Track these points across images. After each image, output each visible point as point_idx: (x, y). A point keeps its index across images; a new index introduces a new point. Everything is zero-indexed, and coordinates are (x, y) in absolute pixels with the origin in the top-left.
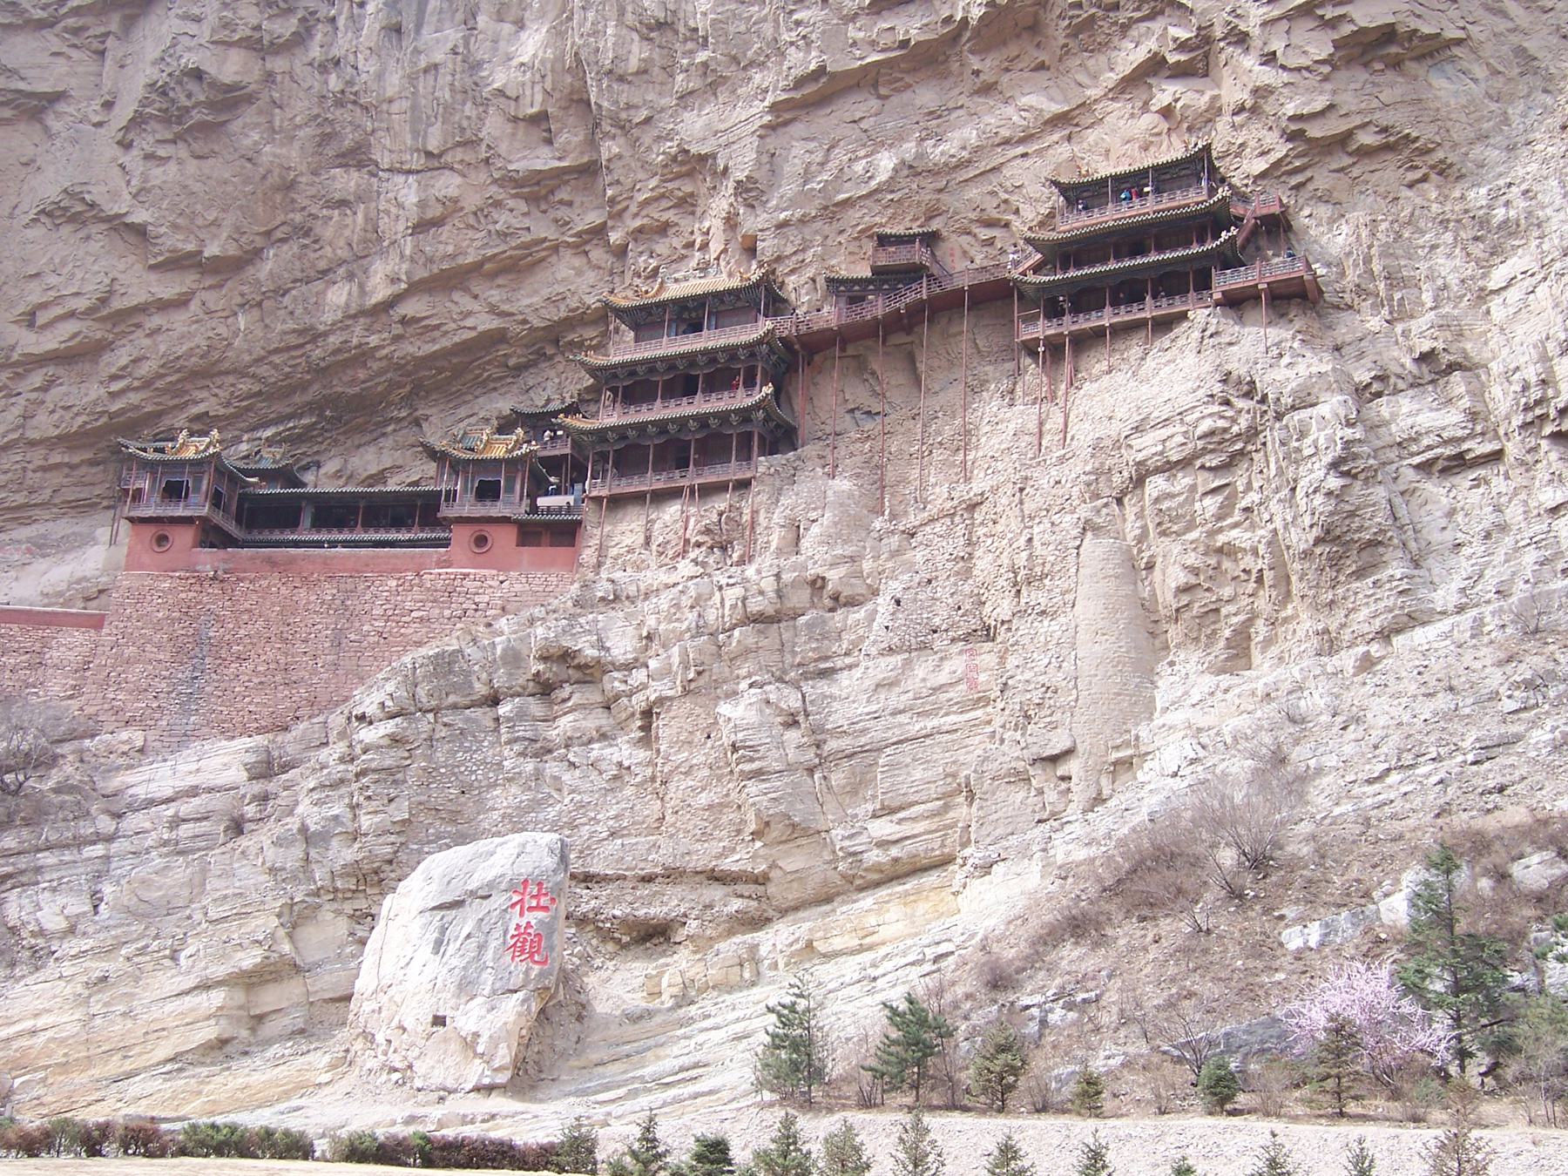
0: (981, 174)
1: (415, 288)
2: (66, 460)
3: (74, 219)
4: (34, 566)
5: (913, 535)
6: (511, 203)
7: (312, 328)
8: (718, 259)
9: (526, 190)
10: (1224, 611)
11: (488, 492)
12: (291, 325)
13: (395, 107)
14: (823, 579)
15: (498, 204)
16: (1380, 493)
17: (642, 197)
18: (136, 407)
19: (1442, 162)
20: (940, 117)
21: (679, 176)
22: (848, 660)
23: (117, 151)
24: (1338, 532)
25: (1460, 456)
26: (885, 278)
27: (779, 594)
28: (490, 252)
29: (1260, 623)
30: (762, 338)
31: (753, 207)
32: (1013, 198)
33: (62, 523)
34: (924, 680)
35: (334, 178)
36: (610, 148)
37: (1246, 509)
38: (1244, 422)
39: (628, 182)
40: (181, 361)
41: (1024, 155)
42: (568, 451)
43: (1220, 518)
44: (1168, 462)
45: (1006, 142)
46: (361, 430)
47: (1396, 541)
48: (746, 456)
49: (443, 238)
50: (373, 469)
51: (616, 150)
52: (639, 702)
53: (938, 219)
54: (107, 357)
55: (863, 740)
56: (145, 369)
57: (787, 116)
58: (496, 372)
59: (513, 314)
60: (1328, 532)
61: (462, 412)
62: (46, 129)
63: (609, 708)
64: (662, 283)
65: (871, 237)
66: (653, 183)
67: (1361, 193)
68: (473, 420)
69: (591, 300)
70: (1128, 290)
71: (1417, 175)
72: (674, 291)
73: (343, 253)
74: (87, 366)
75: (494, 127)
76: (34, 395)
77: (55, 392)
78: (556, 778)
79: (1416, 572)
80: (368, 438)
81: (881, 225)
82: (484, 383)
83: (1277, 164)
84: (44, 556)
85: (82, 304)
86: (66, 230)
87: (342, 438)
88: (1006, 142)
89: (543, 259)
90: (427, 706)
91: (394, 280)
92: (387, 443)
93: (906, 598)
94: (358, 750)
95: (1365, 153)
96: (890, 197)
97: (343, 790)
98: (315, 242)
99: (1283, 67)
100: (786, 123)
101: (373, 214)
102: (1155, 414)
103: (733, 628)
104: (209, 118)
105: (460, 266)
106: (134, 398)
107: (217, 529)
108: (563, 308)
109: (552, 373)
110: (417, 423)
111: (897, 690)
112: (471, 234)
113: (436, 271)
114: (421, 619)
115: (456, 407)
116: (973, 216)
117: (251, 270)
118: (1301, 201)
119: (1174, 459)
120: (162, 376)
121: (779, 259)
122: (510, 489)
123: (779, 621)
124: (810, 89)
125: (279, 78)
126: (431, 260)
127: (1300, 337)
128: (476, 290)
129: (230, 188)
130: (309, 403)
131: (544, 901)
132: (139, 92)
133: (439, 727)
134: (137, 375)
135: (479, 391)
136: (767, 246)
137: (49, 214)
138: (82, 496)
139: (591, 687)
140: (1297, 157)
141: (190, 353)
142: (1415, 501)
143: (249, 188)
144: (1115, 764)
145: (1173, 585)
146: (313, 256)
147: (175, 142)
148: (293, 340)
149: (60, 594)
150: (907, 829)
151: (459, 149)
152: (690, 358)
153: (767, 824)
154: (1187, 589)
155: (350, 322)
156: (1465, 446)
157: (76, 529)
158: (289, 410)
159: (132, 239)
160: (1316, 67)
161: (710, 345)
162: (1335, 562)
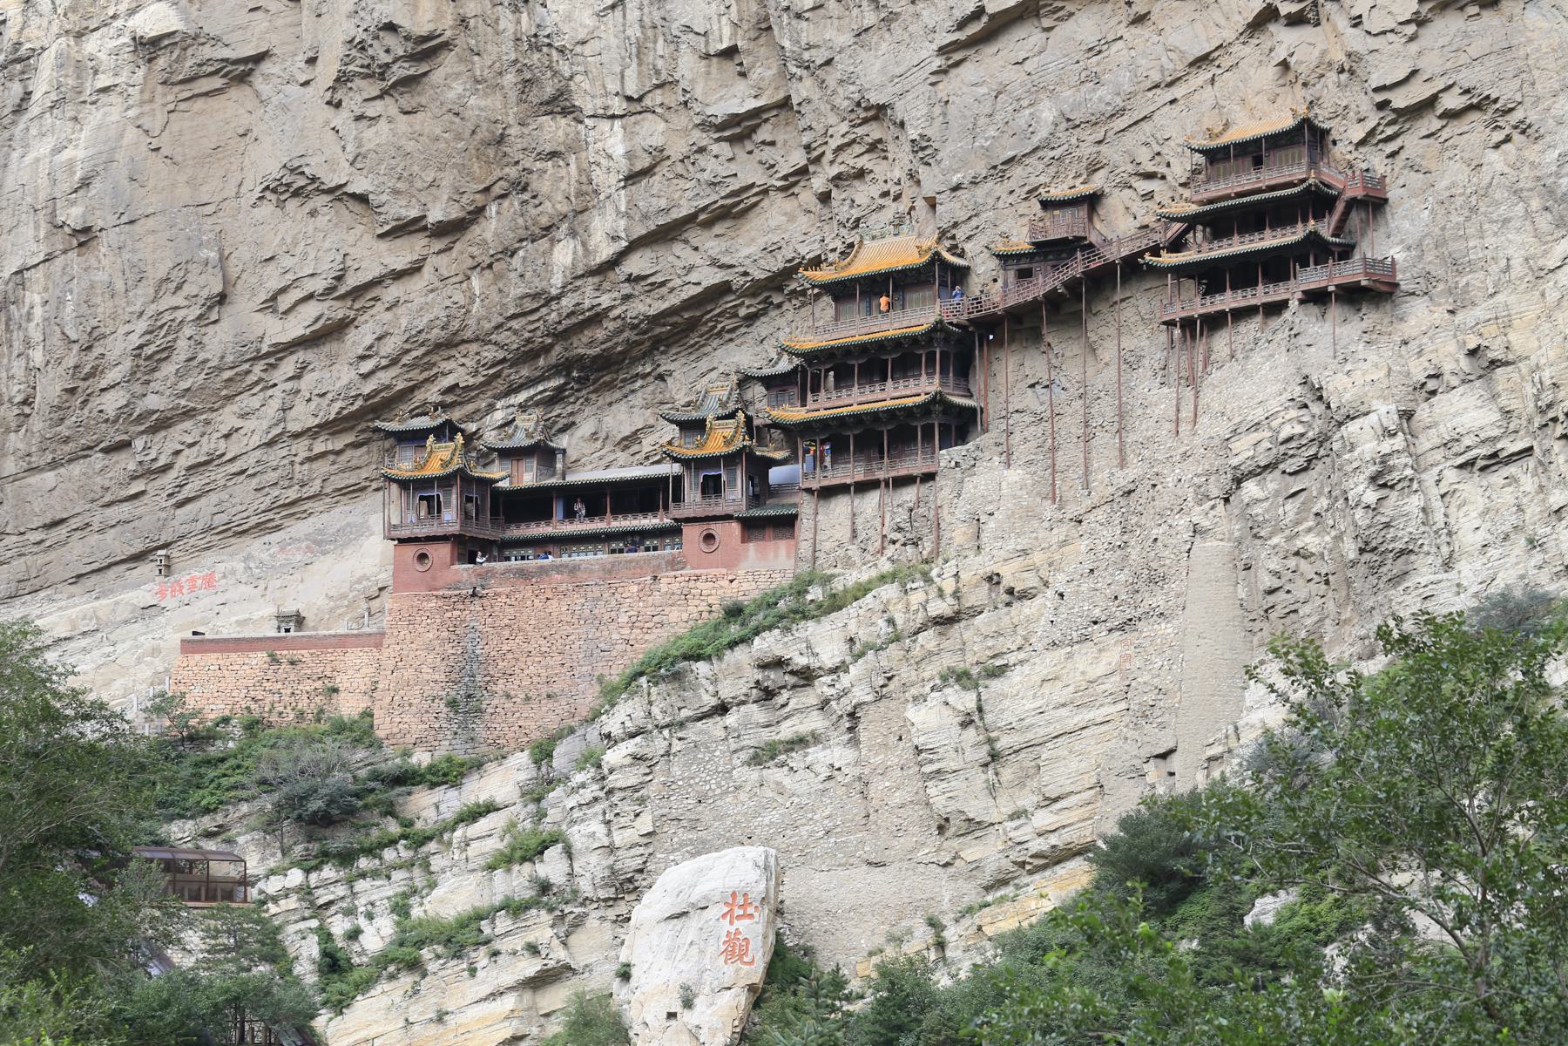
0: (1136, 123)
1: (635, 245)
2: (330, 447)
3: (296, 194)
4: (316, 566)
5: (1080, 522)
6: (715, 148)
8: (909, 213)
9: (727, 134)
10: (1301, 613)
11: (712, 487)
12: (520, 291)
13: (587, 49)
14: (998, 575)
15: (702, 150)
16: (1415, 502)
17: (834, 143)
18: (388, 387)
19: (1522, 122)
20: (1100, 52)
21: (865, 121)
22: (1022, 655)
23: (330, 110)
24: (1374, 544)
25: (1495, 455)
26: (1051, 251)
27: (956, 594)
28: (702, 203)
29: (1327, 621)
32: (1164, 151)
34: (1083, 673)
36: (802, 90)
37: (1317, 514)
38: (1318, 425)
39: (820, 128)
41: (1173, 102)
43: (1298, 523)
44: (1258, 466)
45: (1157, 86)
46: (610, 386)
47: (1426, 548)
51: (804, 94)
52: (845, 705)
53: (1101, 173)
54: (352, 335)
55: (1030, 736)
56: (389, 347)
57: (957, 57)
60: (1367, 543)
61: (704, 365)
62: (258, 95)
66: (844, 127)
67: (1450, 158)
68: (713, 375)
69: (803, 250)
70: (1243, 272)
71: (1498, 136)
73: (564, 208)
75: (688, 66)
76: (288, 386)
77: (309, 379)
78: (778, 784)
79: (1445, 576)
80: (618, 394)
81: (1046, 185)
82: (719, 334)
83: (1372, 133)
84: (324, 553)
85: (319, 285)
86: (292, 204)
87: (593, 397)
88: (1157, 86)
89: (755, 205)
90: (662, 723)
91: (615, 238)
92: (637, 399)
93: (1067, 590)
94: (606, 771)
95: (1451, 115)
96: (1052, 154)
97: (598, 808)
98: (534, 197)
99: (1369, 33)
100: (957, 64)
101: (585, 165)
102: (1249, 418)
104: (411, 72)
106: (384, 377)
108: (780, 257)
109: (781, 322)
110: (661, 377)
111: (1059, 684)
112: (682, 183)
113: (653, 227)
115: (698, 359)
116: (1131, 168)
117: (475, 231)
118: (1397, 169)
119: (1262, 464)
120: (408, 351)
121: (956, 225)
122: (732, 483)
123: (959, 621)
124: (974, 29)
125: (472, 22)
126: (646, 217)
127: (1366, 337)
128: (695, 242)
129: (442, 145)
131: (750, 910)
132: (341, 50)
133: (675, 742)
134: (383, 353)
135: (715, 343)
137: (274, 191)
138: (352, 481)
140: (1391, 123)
142: (1455, 502)
143: (461, 145)
144: (1210, 759)
145: (1262, 588)
146: (534, 212)
147: (380, 97)
149: (344, 596)
150: (1064, 818)
151: (659, 91)
153: (947, 820)
154: (1271, 592)
155: (579, 283)
156: (1499, 446)
157: (350, 519)
158: (538, 373)
159: (357, 207)
160: (1399, 29)
162: (1374, 569)
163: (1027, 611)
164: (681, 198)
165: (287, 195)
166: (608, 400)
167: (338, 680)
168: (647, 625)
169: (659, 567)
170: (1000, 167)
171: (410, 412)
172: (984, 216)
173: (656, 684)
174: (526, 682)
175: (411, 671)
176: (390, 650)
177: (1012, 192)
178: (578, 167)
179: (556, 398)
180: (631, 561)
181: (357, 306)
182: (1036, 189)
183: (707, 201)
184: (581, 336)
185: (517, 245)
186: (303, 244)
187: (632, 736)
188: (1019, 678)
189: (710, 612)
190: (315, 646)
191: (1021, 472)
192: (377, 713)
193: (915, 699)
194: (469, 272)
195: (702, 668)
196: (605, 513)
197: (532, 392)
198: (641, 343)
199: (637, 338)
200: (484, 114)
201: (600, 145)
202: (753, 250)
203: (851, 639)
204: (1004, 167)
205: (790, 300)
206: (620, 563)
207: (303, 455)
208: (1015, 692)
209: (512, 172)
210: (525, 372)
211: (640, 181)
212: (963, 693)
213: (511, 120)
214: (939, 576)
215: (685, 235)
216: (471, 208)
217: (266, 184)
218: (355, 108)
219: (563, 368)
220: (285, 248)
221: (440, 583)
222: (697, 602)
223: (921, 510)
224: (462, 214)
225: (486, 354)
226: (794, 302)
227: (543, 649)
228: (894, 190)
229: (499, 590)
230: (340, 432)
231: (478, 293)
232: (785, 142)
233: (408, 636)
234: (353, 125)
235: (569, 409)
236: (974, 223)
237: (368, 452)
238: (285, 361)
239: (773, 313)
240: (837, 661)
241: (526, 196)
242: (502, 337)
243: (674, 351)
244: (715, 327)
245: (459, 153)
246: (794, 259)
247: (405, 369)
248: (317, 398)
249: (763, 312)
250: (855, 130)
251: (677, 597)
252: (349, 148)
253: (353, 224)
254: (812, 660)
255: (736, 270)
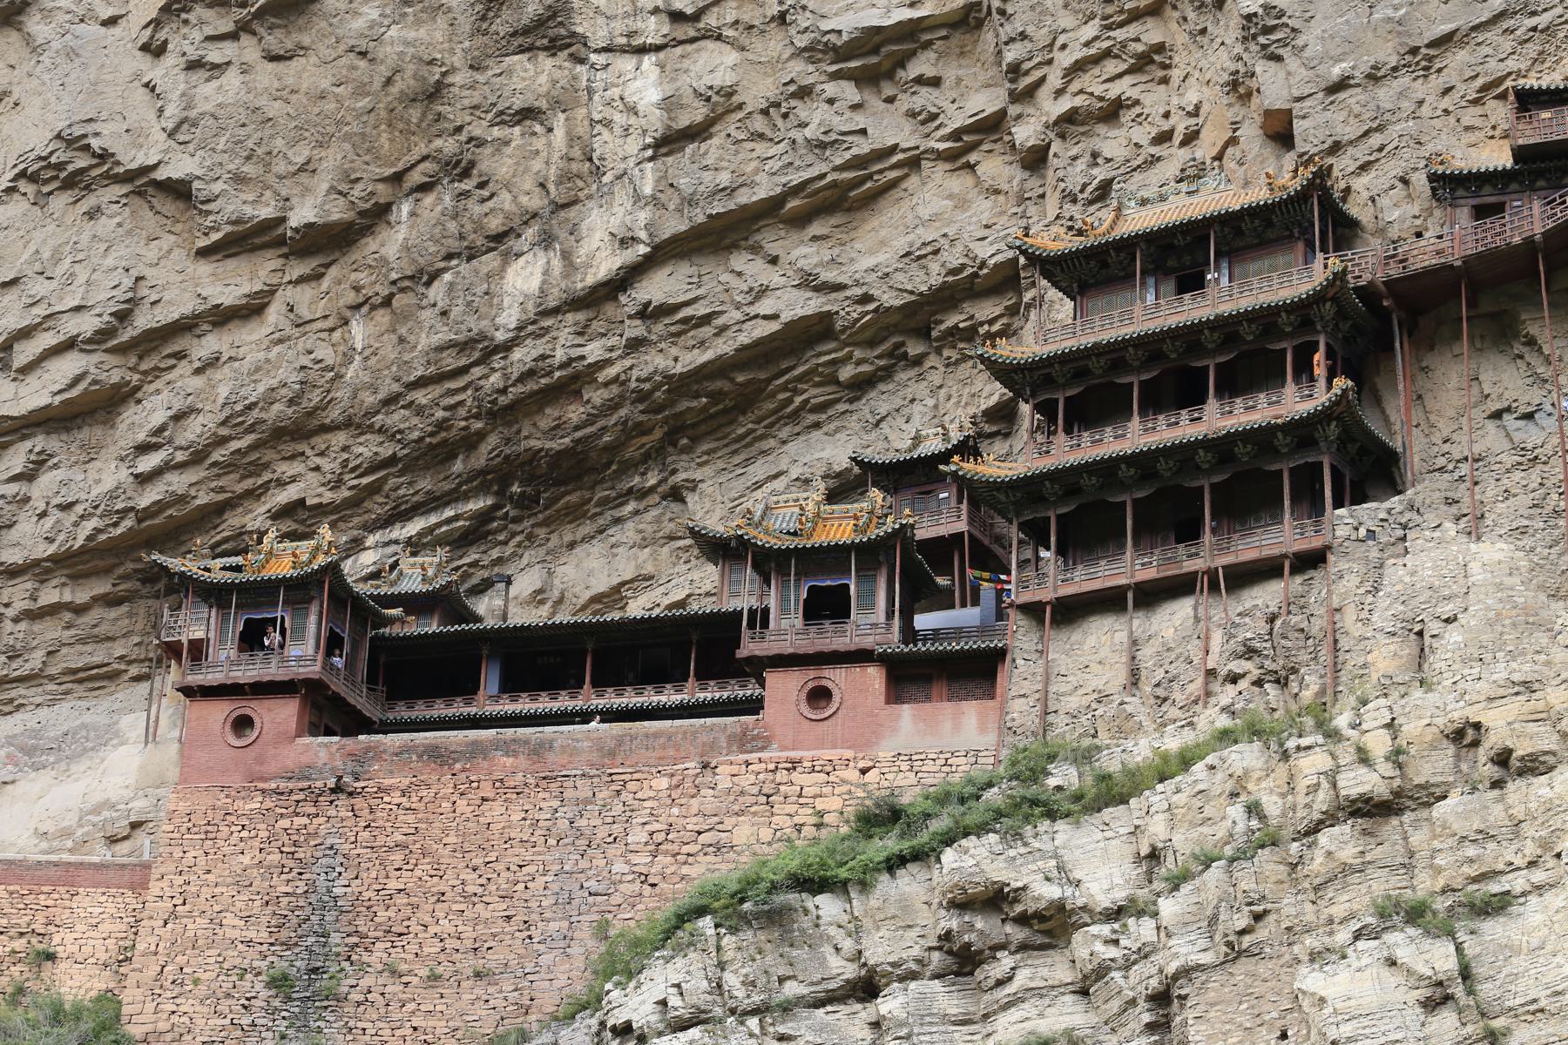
1: (664, 253)
2: (67, 597)
3: (69, 184)
6: (831, 89)
7: (483, 336)
8: (1219, 157)
9: (853, 64)
12: (443, 335)
14: (1477, 726)
15: (804, 93)
17: (1065, 59)
18: (182, 499)
22: (1538, 876)
23: (143, 62)
27: (1396, 756)
28: (796, 178)
30: (1324, 289)
31: (1278, 59)
33: (64, 708)
35: (508, 72)
39: (1041, 36)
40: (255, 413)
42: (962, 526)
46: (575, 514)
48: (1310, 503)
49: (709, 161)
50: (601, 584)
52: (1145, 978)
56: (194, 431)
58: (816, 395)
59: (840, 287)
61: (759, 470)
62: (28, 39)
63: (1084, 993)
64: (1119, 209)
65: (1502, 96)
66: (1090, 30)
68: (779, 484)
72: (1139, 220)
73: (535, 202)
74: (98, 431)
77: (47, 481)
80: (587, 528)
81: (1519, 74)
82: (795, 416)
85: (87, 325)
86: (60, 202)
87: (541, 532)
90: (746, 1004)
91: (626, 242)
98: (482, 185)
101: (582, 129)
103: (1315, 829)
105: (744, 208)
106: (177, 482)
107: (338, 702)
108: (935, 267)
109: (921, 389)
110: (676, 495)
112: (761, 148)
113: (701, 219)
114: (718, 848)
115: (748, 462)
117: (370, 245)
120: (222, 441)
121: (1336, 148)
122: (868, 604)
123: (1399, 812)
126: (691, 201)
128: (772, 248)
129: (330, 106)
130: (482, 472)
134: (180, 441)
135: (784, 434)
136: (1310, 132)
137: (33, 178)
138: (97, 659)
139: (1054, 956)
141: (269, 399)
143: (364, 103)
146: (477, 210)
147: (233, 36)
148: (451, 361)
149: (66, 833)
152: (1189, 336)
157: (88, 718)
158: (447, 486)
159: (169, 206)
161: (1226, 308)
163: (1545, 792)
164: (756, 171)
165: (55, 184)
166: (568, 538)
167: (56, 939)
168: (685, 849)
169: (713, 746)
170: (1424, 51)
171: (213, 548)
172: (1394, 131)
173: (733, 930)
174: (432, 948)
175: (202, 922)
176: (165, 883)
177: (1447, 91)
178: (568, 133)
179: (474, 534)
180: (657, 735)
181: (144, 366)
182: (1501, 80)
183: (806, 175)
184: (537, 418)
185: (442, 265)
186: (69, 260)
187: (681, 1026)
188: (1539, 918)
189: (819, 826)
190: (20, 879)
191: (1505, 546)
192: (126, 997)
193: (1314, 957)
194: (348, 314)
195: (828, 906)
196: (580, 685)
197: (433, 519)
198: (642, 429)
199: (643, 418)
200: (412, 50)
201: (614, 92)
202: (885, 258)
203: (1154, 856)
204: (1432, 52)
205: (939, 351)
206: (633, 738)
207: (20, 605)
208: (1535, 943)
209: (448, 146)
210: (425, 484)
211: (682, 149)
212: (1427, 943)
213: (457, 60)
214: (1354, 727)
215: (758, 237)
216: (368, 206)
217: (21, 167)
218: (189, 50)
219: (495, 478)
220: (38, 267)
221: (272, 767)
222: (791, 809)
223: (1294, 620)
224: (348, 216)
225: (361, 449)
226: (946, 353)
227: (470, 889)
228: (1181, 125)
229: (387, 782)
230: (87, 575)
231: (359, 347)
232: (959, 80)
233: (202, 861)
234: (182, 77)
235: (495, 553)
236: (1375, 140)
237: (130, 615)
238: (11, 450)
239: (902, 376)
240: (1120, 895)
241: (467, 185)
242: (396, 418)
243: (705, 447)
244: (790, 401)
245: (358, 117)
246: (963, 267)
247: (216, 470)
248: (55, 511)
249: (885, 374)
250: (1111, 34)
251: (750, 800)
252: (167, 113)
253: (158, 232)
254: (1069, 891)
255: (848, 293)
